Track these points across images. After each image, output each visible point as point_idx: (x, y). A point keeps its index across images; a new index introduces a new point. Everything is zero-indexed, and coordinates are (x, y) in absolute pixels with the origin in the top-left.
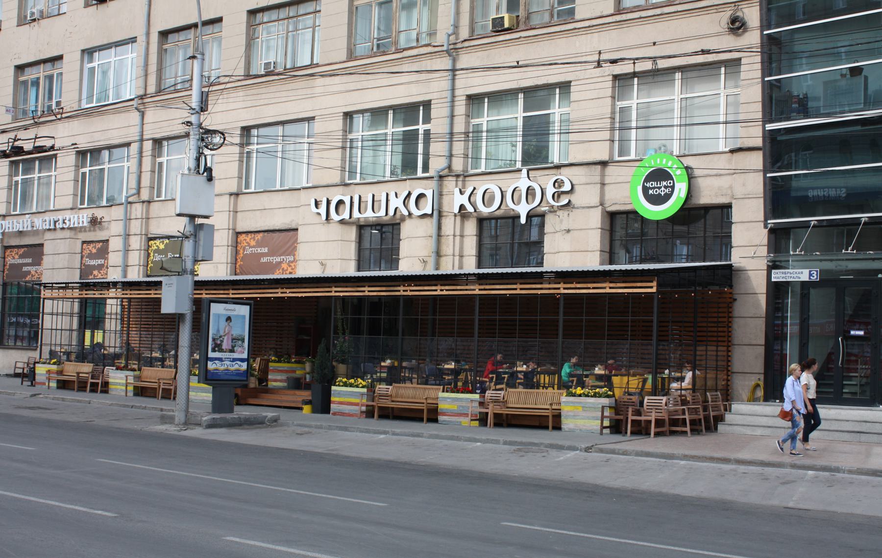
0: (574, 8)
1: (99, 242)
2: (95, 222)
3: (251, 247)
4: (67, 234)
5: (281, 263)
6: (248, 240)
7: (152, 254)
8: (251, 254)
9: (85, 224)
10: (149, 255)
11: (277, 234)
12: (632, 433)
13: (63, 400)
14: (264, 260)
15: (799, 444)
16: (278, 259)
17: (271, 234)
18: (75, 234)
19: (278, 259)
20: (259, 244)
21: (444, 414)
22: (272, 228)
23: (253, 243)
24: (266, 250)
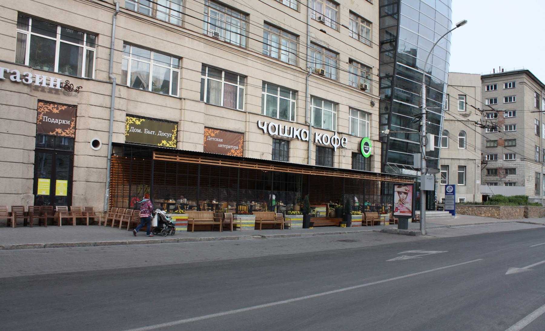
0: (437, 160)
1: (63, 105)
2: (67, 88)
3: (211, 137)
4: (26, 89)
5: (230, 149)
6: (210, 132)
7: (173, 138)
8: (212, 141)
9: (58, 87)
10: (176, 138)
11: (229, 133)
12: (62, 225)
13: (282, 236)
14: (220, 146)
15: (114, 218)
16: (229, 147)
17: (225, 132)
18: (31, 91)
19: (229, 147)
20: (216, 136)
21: (185, 224)
22: (227, 129)
23: (213, 135)
24: (222, 140)
